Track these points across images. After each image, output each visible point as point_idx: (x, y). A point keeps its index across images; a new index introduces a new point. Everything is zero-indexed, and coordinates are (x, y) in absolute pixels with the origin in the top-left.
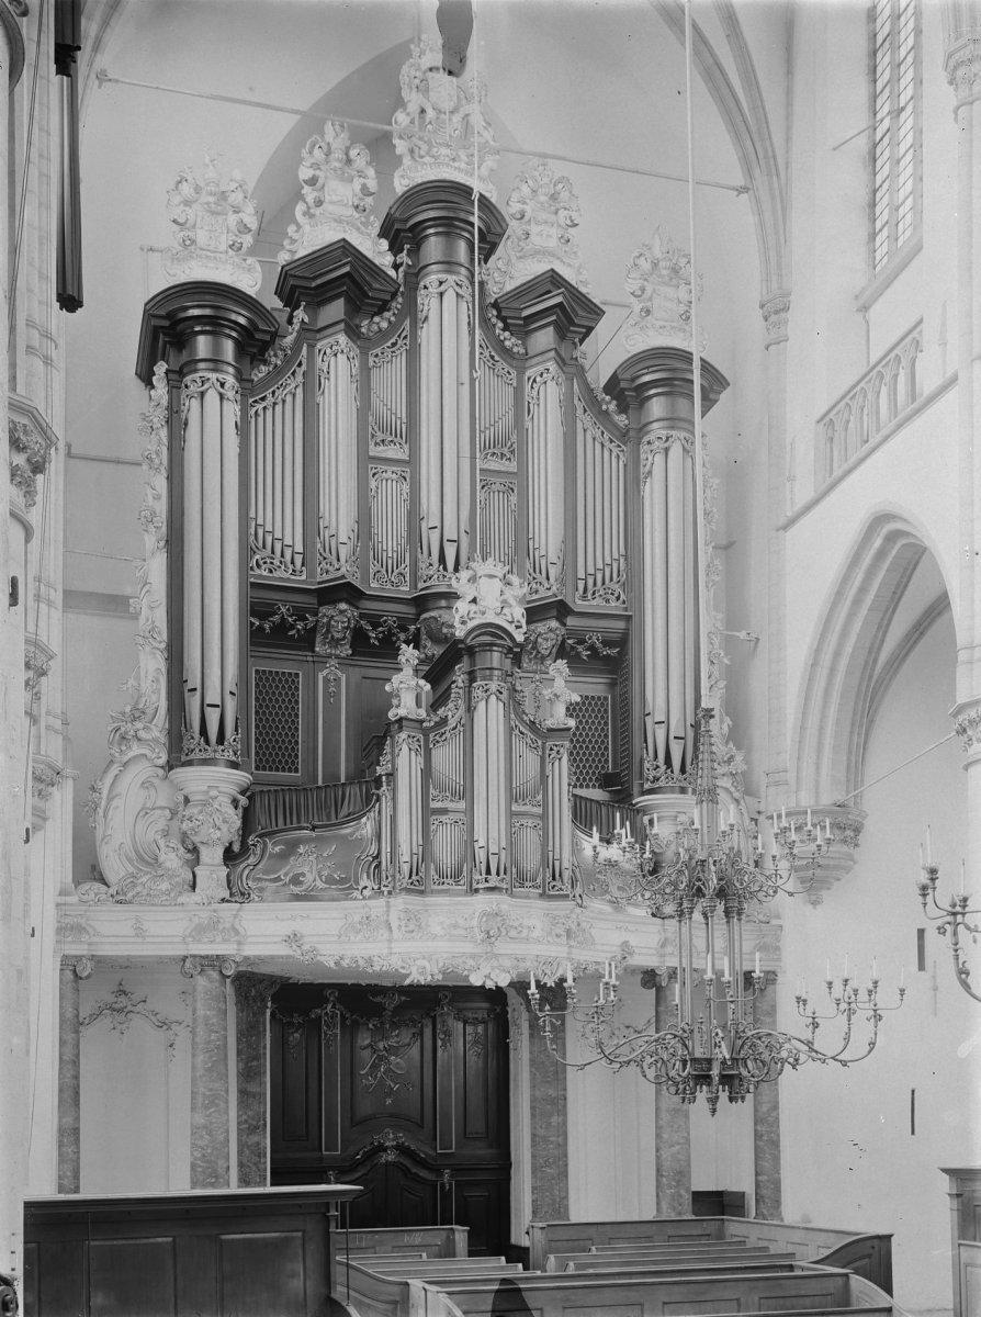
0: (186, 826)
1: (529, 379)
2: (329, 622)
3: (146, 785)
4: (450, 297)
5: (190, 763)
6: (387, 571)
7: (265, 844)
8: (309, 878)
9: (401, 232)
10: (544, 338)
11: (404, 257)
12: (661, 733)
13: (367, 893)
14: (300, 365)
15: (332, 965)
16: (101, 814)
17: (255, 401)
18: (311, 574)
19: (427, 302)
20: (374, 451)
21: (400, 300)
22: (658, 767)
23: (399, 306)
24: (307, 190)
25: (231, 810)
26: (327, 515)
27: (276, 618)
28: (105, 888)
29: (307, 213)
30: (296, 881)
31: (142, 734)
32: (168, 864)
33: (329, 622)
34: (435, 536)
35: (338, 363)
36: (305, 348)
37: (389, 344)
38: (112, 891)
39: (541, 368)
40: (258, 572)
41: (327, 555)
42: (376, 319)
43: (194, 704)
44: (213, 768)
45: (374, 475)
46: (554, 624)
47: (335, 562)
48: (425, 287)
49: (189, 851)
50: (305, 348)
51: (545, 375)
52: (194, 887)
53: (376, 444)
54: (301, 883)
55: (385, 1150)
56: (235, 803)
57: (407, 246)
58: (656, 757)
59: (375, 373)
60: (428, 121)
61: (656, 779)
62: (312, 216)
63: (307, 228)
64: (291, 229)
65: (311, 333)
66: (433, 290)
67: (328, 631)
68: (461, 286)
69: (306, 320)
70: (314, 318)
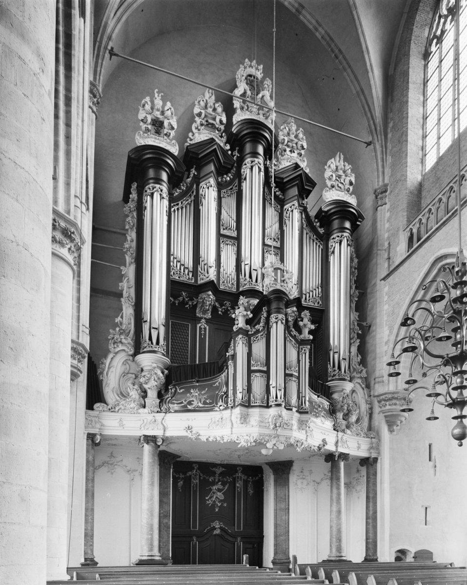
0: (142, 380)
1: (285, 209)
2: (203, 301)
3: (125, 363)
4: (256, 169)
5: (144, 352)
6: (227, 282)
7: (176, 388)
8: (195, 403)
9: (236, 141)
10: (294, 191)
11: (236, 153)
12: (336, 356)
13: (222, 408)
14: (193, 192)
15: (205, 440)
16: (105, 374)
17: (174, 205)
18: (196, 280)
19: (245, 171)
20: (222, 232)
21: (235, 169)
22: (335, 370)
23: (234, 172)
24: (197, 119)
25: (161, 375)
26: (203, 256)
27: (181, 299)
28: (105, 405)
29: (197, 128)
30: (190, 403)
31: (123, 341)
32: (134, 396)
33: (203, 301)
34: (247, 268)
35: (210, 194)
36: (195, 186)
37: (229, 188)
38: (109, 407)
39: (291, 204)
40: (174, 277)
41: (203, 272)
42: (225, 176)
43: (146, 328)
44: (154, 354)
45: (223, 242)
46: (295, 309)
47: (206, 275)
48: (245, 164)
49: (143, 392)
50: (195, 186)
51: (292, 207)
52: (144, 407)
53: (224, 229)
54: (192, 404)
55: (216, 529)
56: (163, 373)
57: (237, 148)
58: (334, 366)
59: (223, 200)
60: (247, 96)
61: (334, 375)
62: (199, 130)
63: (196, 135)
64: (190, 135)
65: (197, 180)
66: (249, 165)
67: (202, 306)
68: (260, 164)
69: (196, 174)
70: (199, 173)
